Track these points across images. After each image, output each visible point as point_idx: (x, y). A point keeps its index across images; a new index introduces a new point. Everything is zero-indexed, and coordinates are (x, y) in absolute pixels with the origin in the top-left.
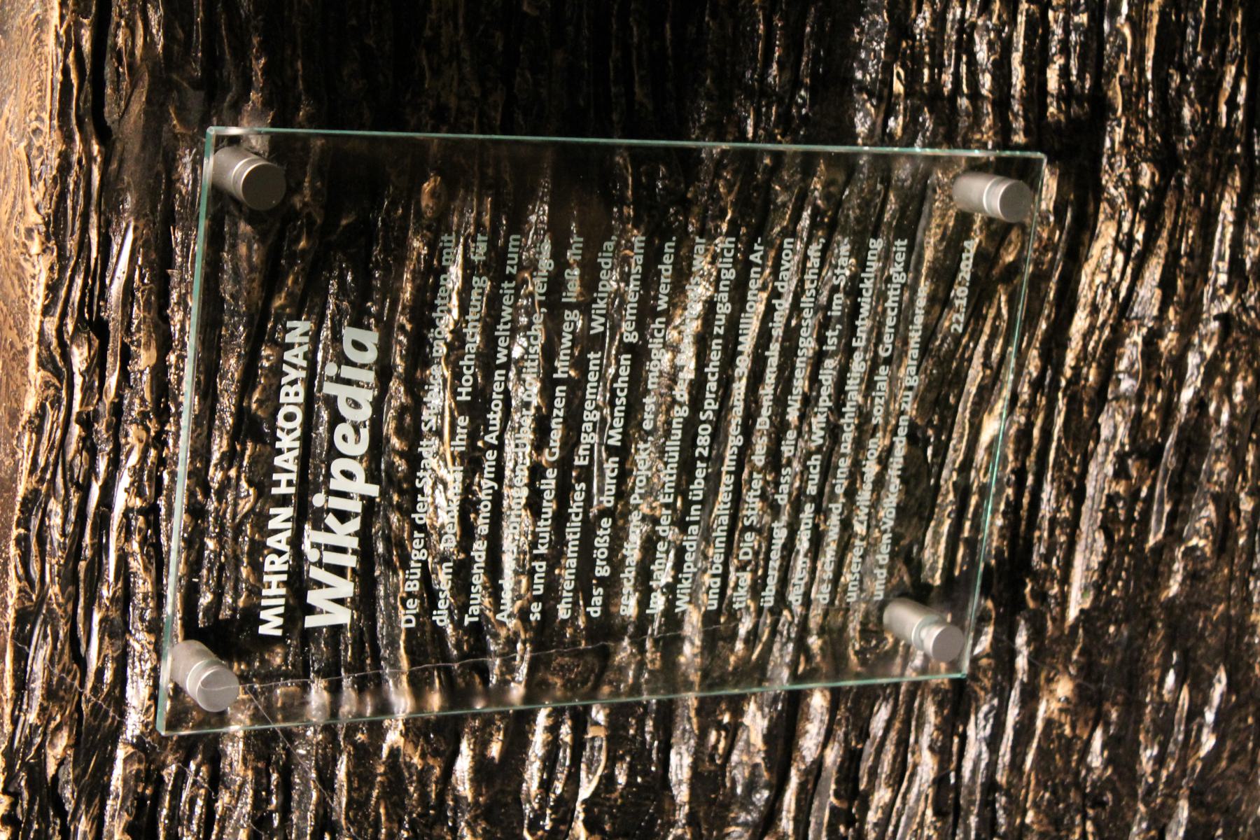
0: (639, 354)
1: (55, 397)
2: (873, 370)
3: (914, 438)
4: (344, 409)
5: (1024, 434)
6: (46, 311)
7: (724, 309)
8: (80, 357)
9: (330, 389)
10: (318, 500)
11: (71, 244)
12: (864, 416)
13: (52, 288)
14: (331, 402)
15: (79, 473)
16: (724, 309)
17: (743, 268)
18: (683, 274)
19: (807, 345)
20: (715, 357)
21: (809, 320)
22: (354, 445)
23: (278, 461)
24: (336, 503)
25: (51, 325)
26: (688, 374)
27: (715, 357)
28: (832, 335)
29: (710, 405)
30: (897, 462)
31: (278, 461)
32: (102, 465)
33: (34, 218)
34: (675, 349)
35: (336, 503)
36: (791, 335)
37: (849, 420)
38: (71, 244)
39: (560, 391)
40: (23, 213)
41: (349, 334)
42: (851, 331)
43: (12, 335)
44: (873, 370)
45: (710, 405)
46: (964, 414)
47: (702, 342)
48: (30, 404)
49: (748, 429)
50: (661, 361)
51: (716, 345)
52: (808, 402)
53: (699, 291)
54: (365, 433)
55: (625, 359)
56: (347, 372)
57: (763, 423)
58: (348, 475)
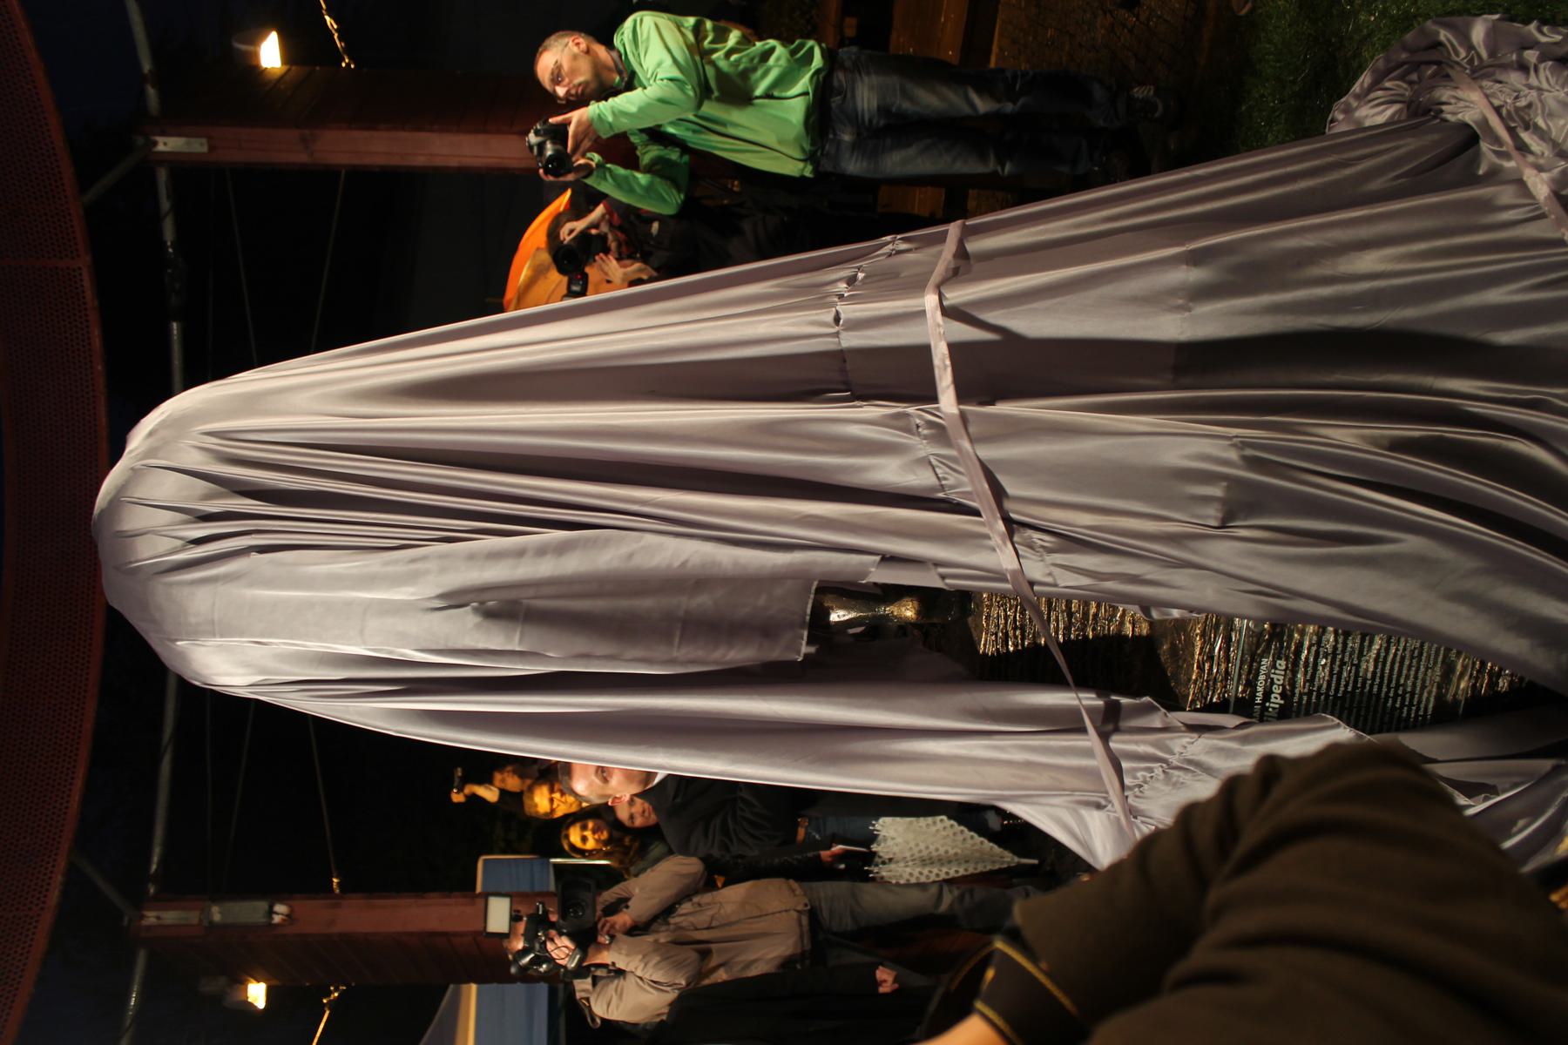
0: (1358, 666)
1: (1200, 675)
2: (1426, 671)
3: (1439, 687)
4: (1276, 681)
5: (1474, 685)
6: (1200, 654)
7: (1383, 654)
8: (1207, 666)
9: (1272, 676)
10: (1267, 704)
11: (1207, 638)
12: (1424, 681)
13: (1201, 649)
14: (1272, 679)
15: (1204, 694)
16: (1383, 654)
17: (1389, 642)
18: (1371, 643)
19: (1407, 662)
20: (1380, 667)
21: (1408, 654)
22: (1277, 690)
23: (1258, 694)
24: (1272, 705)
25: (1201, 658)
26: (1371, 669)
27: (1380, 667)
28: (1415, 661)
29: (1378, 680)
30: (1434, 694)
31: (1258, 694)
32: (1210, 693)
33: (1198, 631)
34: (1368, 662)
35: (1272, 705)
36: (1403, 658)
37: (1419, 683)
38: (1207, 638)
39: (1335, 676)
40: (1195, 630)
41: (1278, 662)
42: (1420, 660)
43: (1190, 659)
44: (1426, 671)
45: (1378, 680)
46: (1455, 679)
47: (1376, 660)
48: (1194, 677)
49: (1389, 687)
50: (1364, 666)
51: (1380, 664)
52: (1407, 677)
53: (1376, 647)
54: (1281, 687)
55: (1354, 668)
56: (1277, 672)
57: (1393, 685)
58: (1276, 698)
